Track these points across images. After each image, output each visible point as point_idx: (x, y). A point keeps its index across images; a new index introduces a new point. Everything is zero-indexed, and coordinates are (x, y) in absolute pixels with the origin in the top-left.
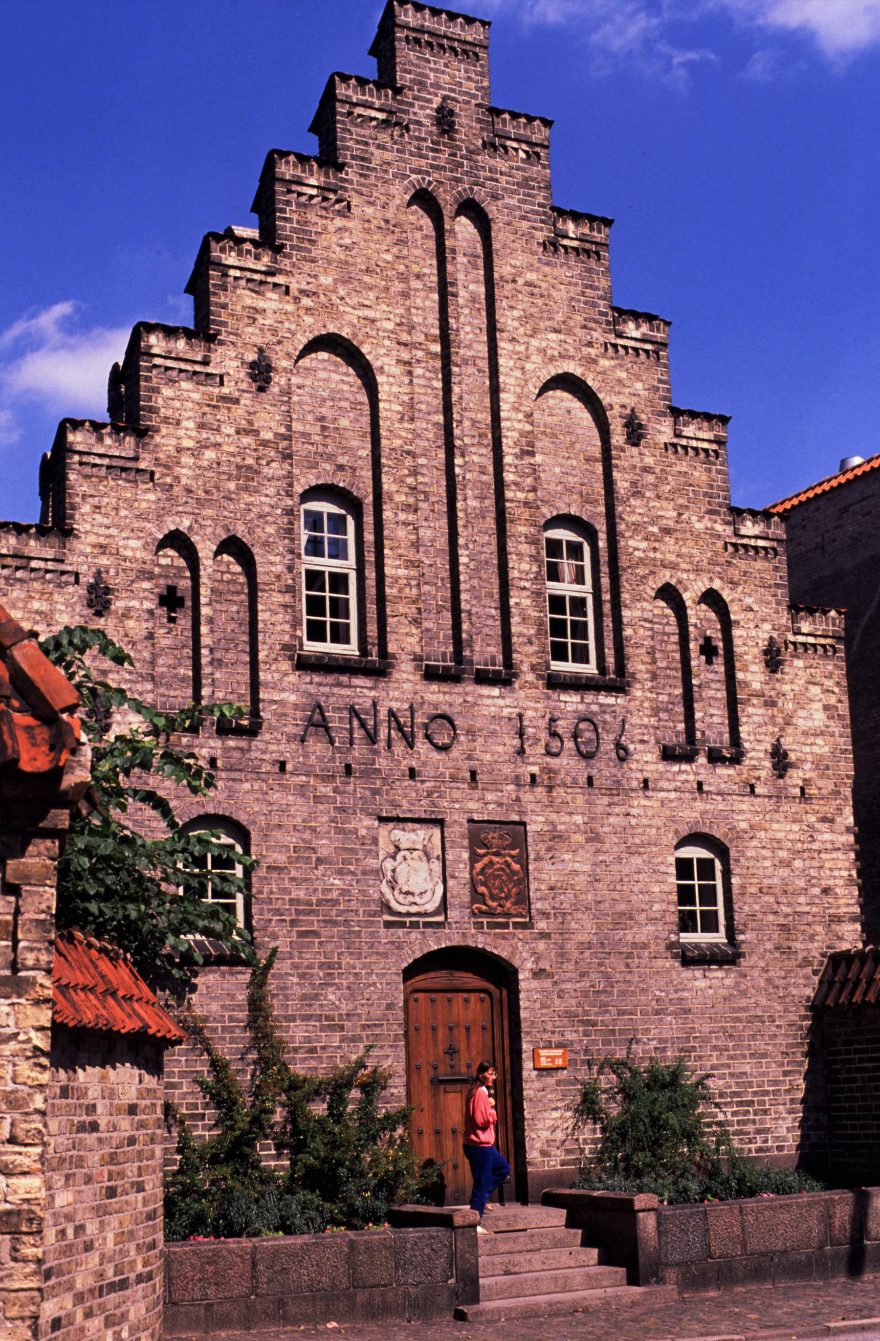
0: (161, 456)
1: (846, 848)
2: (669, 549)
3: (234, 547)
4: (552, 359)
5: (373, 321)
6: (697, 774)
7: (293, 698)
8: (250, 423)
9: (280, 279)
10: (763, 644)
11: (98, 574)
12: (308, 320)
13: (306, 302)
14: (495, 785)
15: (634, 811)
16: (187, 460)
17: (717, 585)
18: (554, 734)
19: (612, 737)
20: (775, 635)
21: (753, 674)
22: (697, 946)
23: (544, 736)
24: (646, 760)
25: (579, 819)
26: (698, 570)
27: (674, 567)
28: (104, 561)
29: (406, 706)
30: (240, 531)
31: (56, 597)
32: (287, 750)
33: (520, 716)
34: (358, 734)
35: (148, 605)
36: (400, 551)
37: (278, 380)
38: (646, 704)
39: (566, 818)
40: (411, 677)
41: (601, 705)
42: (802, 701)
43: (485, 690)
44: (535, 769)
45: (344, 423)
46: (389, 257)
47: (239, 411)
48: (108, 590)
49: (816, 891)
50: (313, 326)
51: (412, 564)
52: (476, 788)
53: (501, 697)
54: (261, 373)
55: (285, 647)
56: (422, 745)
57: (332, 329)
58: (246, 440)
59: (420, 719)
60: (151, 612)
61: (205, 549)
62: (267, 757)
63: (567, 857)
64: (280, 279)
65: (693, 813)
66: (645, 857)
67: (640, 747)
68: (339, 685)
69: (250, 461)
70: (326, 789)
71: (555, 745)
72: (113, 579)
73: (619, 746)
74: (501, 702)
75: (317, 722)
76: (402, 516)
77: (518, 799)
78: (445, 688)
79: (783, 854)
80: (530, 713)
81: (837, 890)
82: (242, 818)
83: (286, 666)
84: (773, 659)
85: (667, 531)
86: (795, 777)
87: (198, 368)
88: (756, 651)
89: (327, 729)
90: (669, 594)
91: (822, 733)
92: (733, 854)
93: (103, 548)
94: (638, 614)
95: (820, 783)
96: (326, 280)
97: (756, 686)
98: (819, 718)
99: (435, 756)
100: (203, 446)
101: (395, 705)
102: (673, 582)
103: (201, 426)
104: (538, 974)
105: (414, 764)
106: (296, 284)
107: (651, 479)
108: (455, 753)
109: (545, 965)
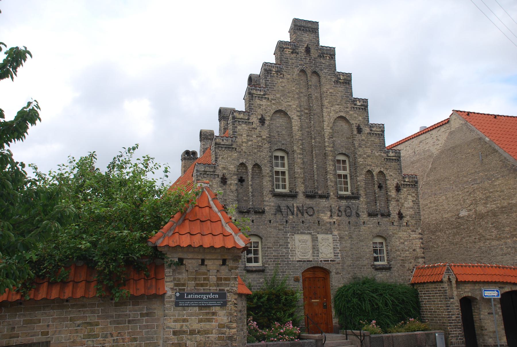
0: (238, 144)
2: (369, 161)
3: (257, 166)
4: (337, 112)
5: (290, 106)
7: (272, 204)
8: (260, 134)
9: (266, 96)
10: (395, 185)
11: (223, 175)
12: (274, 106)
13: (273, 102)
14: (324, 225)
15: (361, 230)
16: (244, 144)
17: (382, 170)
18: (340, 211)
21: (393, 193)
22: (379, 265)
23: (337, 212)
24: (364, 216)
25: (347, 233)
26: (377, 166)
27: (371, 165)
28: (225, 171)
30: (258, 162)
32: (272, 217)
34: (289, 213)
35: (236, 182)
37: (267, 123)
39: (343, 232)
42: (406, 199)
44: (335, 220)
45: (284, 132)
46: (294, 88)
47: (257, 131)
48: (226, 179)
49: (411, 250)
50: (275, 108)
51: (301, 168)
53: (326, 202)
54: (262, 121)
55: (270, 191)
56: (306, 215)
57: (280, 108)
58: (259, 139)
60: (236, 184)
61: (250, 167)
64: (266, 96)
68: (284, 200)
69: (260, 144)
70: (281, 227)
72: (228, 176)
75: (279, 210)
76: (299, 156)
77: (331, 228)
79: (402, 241)
80: (333, 206)
82: (260, 235)
83: (270, 196)
84: (398, 189)
85: (368, 156)
86: (405, 220)
87: (246, 121)
89: (281, 212)
90: (369, 172)
91: (412, 208)
92: (388, 241)
93: (224, 168)
95: (412, 221)
96: (278, 96)
99: (309, 217)
100: (248, 141)
104: (337, 273)
106: (271, 97)
107: (364, 142)
108: (314, 217)
109: (339, 271)
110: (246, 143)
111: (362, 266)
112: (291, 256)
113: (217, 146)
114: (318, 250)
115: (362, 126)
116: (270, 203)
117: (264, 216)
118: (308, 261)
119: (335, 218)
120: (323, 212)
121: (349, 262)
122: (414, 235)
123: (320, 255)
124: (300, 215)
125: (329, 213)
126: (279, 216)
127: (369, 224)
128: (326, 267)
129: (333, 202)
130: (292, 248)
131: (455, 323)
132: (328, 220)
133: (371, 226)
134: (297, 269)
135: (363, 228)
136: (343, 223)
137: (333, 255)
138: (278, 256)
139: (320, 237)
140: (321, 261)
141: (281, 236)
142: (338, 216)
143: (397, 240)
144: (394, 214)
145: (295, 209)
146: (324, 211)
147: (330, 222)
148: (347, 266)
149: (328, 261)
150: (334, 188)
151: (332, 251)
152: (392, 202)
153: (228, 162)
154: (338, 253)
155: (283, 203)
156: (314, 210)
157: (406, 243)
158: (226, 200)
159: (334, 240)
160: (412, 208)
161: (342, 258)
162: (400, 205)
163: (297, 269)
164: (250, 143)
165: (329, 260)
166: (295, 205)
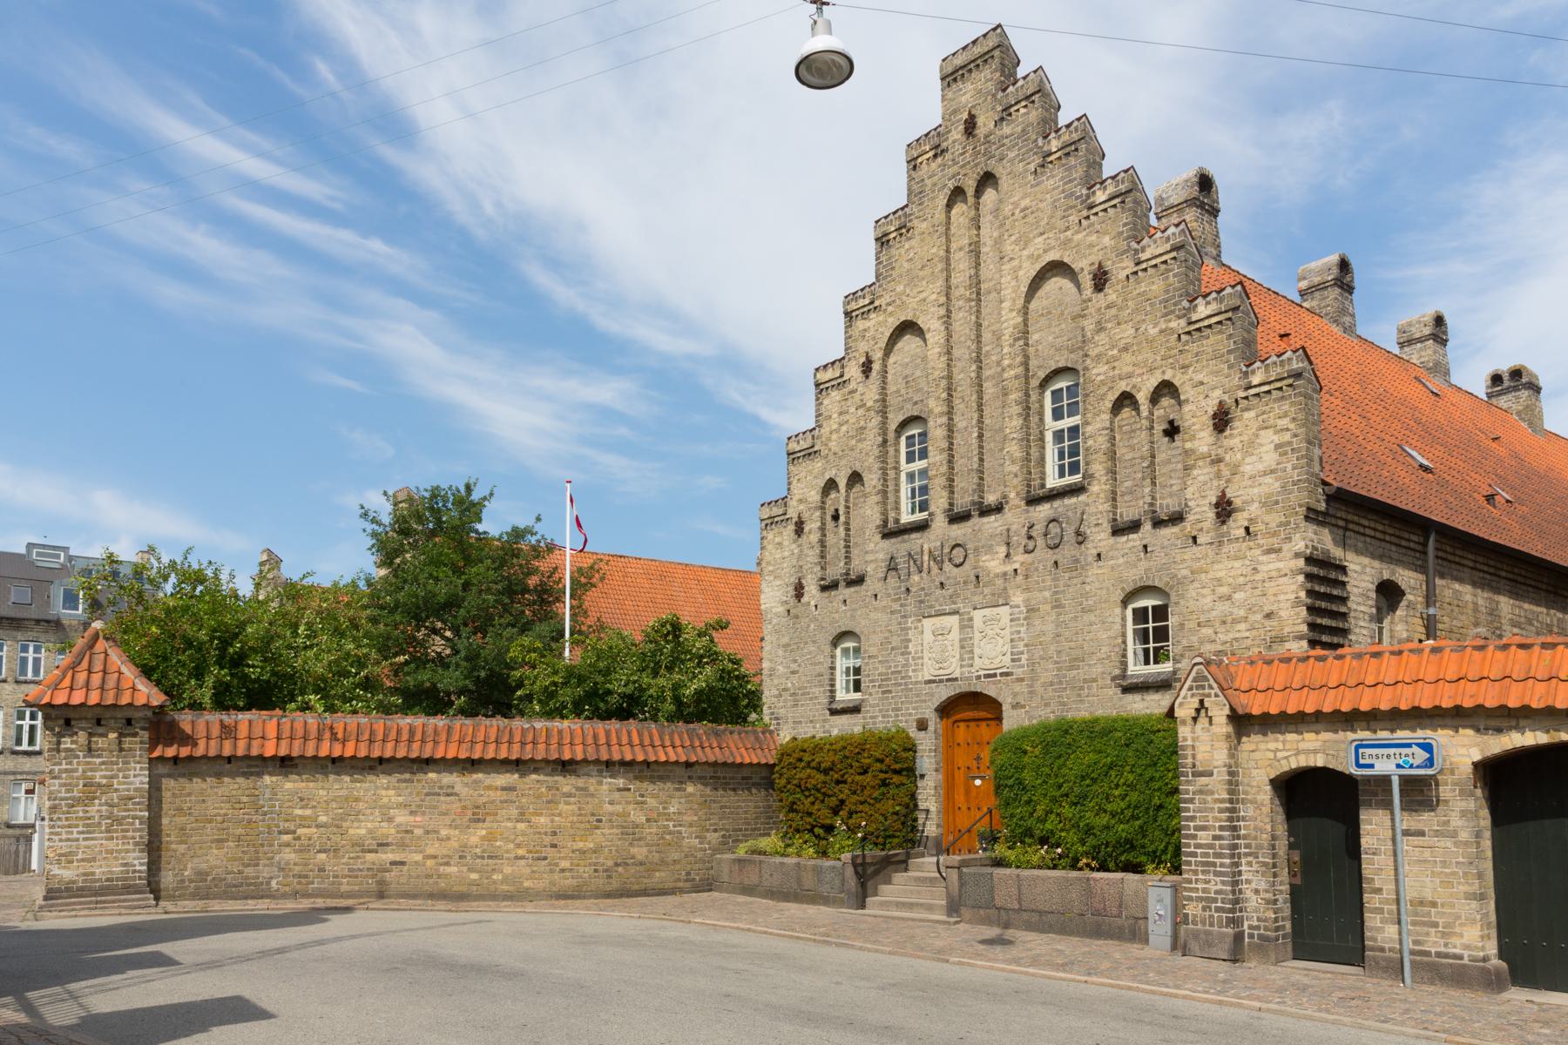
1: (1295, 573)
14: (990, 583)
18: (1030, 538)
20: (1226, 397)
23: (1024, 541)
24: (1100, 537)
25: (1047, 594)
27: (1129, 376)
39: (1038, 595)
43: (985, 520)
44: (1017, 566)
47: (857, 396)
49: (1258, 617)
56: (947, 566)
58: (861, 412)
59: (946, 550)
65: (1135, 575)
70: (896, 606)
71: (1031, 545)
72: (805, 516)
73: (1078, 533)
75: (892, 566)
78: (962, 525)
79: (1224, 590)
80: (1014, 527)
81: (1283, 614)
84: (1221, 420)
85: (1125, 349)
88: (1204, 418)
91: (1272, 472)
94: (1099, 426)
95: (1267, 518)
97: (1204, 449)
98: (1270, 458)
99: (956, 570)
104: (1016, 706)
108: (967, 566)
111: (1085, 681)
114: (972, 652)
116: (873, 553)
119: (1019, 558)
120: (990, 549)
121: (1047, 673)
122: (1270, 565)
123: (977, 662)
124: (935, 570)
125: (1003, 550)
126: (892, 581)
128: (991, 691)
129: (1015, 517)
132: (1001, 569)
133: (1121, 561)
135: (1095, 571)
137: (1008, 657)
139: (978, 616)
140: (979, 677)
141: (894, 628)
142: (1027, 552)
143: (1204, 591)
144: (1202, 511)
145: (926, 558)
147: (1005, 574)
148: (1044, 685)
149: (995, 675)
151: (1007, 648)
152: (1195, 472)
155: (899, 546)
157: (1238, 596)
160: (1272, 472)
162: (1226, 472)
164: (844, 428)
166: (926, 547)
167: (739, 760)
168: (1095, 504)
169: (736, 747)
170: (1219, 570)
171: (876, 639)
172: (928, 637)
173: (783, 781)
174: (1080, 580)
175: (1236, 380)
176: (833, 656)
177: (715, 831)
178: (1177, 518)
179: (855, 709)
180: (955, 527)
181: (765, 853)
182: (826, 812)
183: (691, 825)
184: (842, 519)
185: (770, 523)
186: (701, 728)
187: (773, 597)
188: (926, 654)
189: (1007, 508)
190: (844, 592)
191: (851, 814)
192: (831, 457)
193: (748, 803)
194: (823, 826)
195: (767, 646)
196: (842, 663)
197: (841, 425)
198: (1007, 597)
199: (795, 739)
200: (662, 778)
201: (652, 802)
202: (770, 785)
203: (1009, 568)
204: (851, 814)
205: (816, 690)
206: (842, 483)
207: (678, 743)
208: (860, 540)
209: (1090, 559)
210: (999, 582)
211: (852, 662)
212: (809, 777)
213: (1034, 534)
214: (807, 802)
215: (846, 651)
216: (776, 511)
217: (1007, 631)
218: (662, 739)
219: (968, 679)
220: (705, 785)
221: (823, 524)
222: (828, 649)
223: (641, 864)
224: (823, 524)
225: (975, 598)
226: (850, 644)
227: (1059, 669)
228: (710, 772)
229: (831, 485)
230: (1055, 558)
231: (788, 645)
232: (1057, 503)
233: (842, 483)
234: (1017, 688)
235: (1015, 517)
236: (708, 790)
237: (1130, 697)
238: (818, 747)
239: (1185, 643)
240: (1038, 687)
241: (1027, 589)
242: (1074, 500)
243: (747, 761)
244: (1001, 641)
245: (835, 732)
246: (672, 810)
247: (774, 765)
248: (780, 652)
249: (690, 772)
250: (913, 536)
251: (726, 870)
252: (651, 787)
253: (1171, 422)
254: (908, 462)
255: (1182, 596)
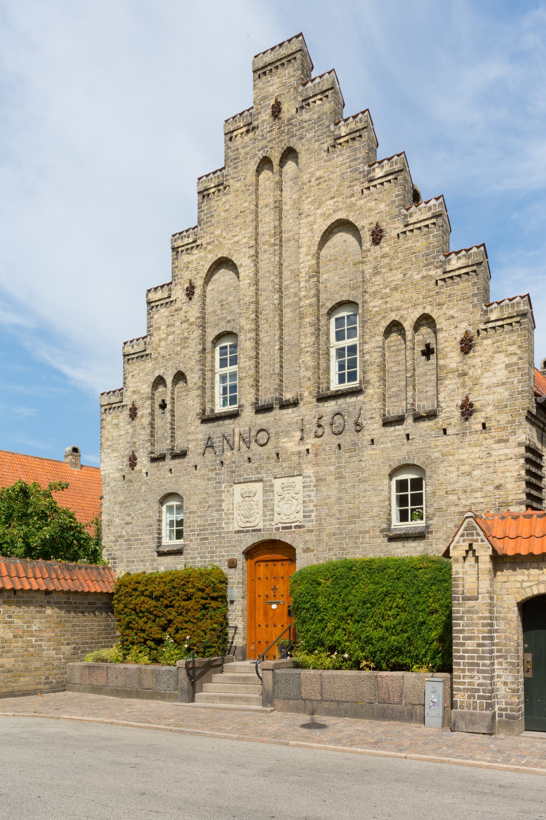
1: (518, 457)
4: (330, 215)
5: (238, 242)
6: (405, 430)
8: (186, 317)
9: (199, 242)
13: (210, 247)
14: (288, 459)
15: (364, 459)
18: (319, 426)
19: (353, 420)
20: (470, 328)
23: (315, 428)
24: (374, 428)
25: (332, 468)
28: (135, 397)
29: (247, 428)
31: (120, 417)
33: (302, 420)
34: (226, 446)
36: (247, 353)
38: (375, 397)
39: (325, 469)
40: (250, 414)
41: (349, 403)
43: (284, 411)
44: (309, 447)
47: (182, 313)
49: (491, 488)
52: (279, 462)
53: (293, 412)
54: (190, 292)
56: (254, 446)
57: (220, 255)
58: (185, 325)
59: (253, 433)
62: (190, 465)
63: (324, 489)
66: (370, 483)
67: (369, 422)
69: (186, 334)
70: (212, 475)
72: (138, 404)
73: (357, 424)
74: (293, 415)
75: (209, 445)
77: (299, 463)
78: (266, 415)
79: (466, 468)
80: (307, 418)
81: (508, 486)
84: (467, 345)
87: (167, 300)
88: (454, 343)
91: (503, 384)
93: (134, 392)
94: (374, 345)
96: (218, 232)
97: (454, 366)
98: (502, 374)
99: (260, 449)
101: (242, 430)
102: (397, 319)
103: (168, 326)
105: (250, 456)
107: (387, 260)
108: (269, 446)
110: (165, 339)
111: (360, 532)
112: (226, 523)
113: (127, 358)
114: (272, 510)
115: (383, 225)
116: (193, 434)
117: (186, 459)
118: (254, 531)
119: (310, 442)
120: (287, 434)
121: (331, 526)
122: (500, 451)
123: (277, 518)
124: (244, 448)
125: (298, 435)
126: (209, 455)
127: (383, 443)
128: (287, 539)
129: (308, 410)
130: (228, 510)
131: (472, 658)
132: (296, 449)
133: (389, 445)
134: (235, 546)
135: (369, 452)
136: (324, 450)
137: (301, 514)
138: (205, 525)
140: (278, 529)
142: (316, 436)
143: (451, 469)
144: (450, 410)
145: (237, 439)
146: (289, 431)
147: (299, 452)
149: (290, 527)
150: (312, 382)
151: (301, 507)
152: (446, 382)
153: (139, 381)
154: (312, 511)
155: (216, 430)
156: (269, 434)
157: (476, 473)
158: (135, 443)
159: (304, 487)
160: (503, 384)
161: (319, 519)
162: (469, 383)
163: (235, 546)
164: (171, 338)
165: (293, 525)
166: (237, 431)
167: (86, 590)
168: (370, 404)
169: (82, 579)
170: (463, 454)
171: (196, 499)
172: (237, 498)
173: (121, 606)
174: (357, 458)
175: (478, 316)
176: (160, 512)
177: (68, 644)
178: (432, 415)
179: (179, 552)
180: (260, 416)
181: (106, 661)
182: (156, 629)
183: (49, 640)
184: (169, 407)
185: (109, 408)
186: (55, 563)
187: (111, 465)
188: (235, 512)
189: (301, 403)
190: (169, 463)
191: (177, 631)
192: (160, 359)
193: (93, 623)
194: (153, 640)
195: (106, 503)
196: (166, 518)
197: (168, 335)
198: (301, 470)
199: (128, 574)
200: (27, 603)
201: (18, 622)
202: (109, 609)
203: (303, 448)
204: (177, 631)
205: (146, 538)
206: (169, 380)
207: (39, 575)
208: (182, 424)
209: (365, 443)
210: (295, 458)
211: (175, 517)
212: (143, 602)
213: (323, 423)
214: (141, 622)
215: (170, 509)
216: (114, 399)
217: (300, 496)
218: (26, 572)
219: (268, 530)
220: (61, 608)
221: (153, 411)
222: (156, 506)
223: (9, 671)
224: (153, 411)
225: (276, 470)
226: (174, 503)
227: (340, 524)
228: (64, 598)
229: (160, 381)
230: (338, 441)
231: (123, 502)
232: (341, 401)
233: (169, 380)
234: (308, 537)
235: (308, 410)
236: (63, 613)
237: (394, 544)
238: (150, 580)
239: (436, 505)
240: (324, 536)
241: (317, 464)
242: (354, 399)
243: (93, 590)
244: (295, 502)
245: (162, 569)
246: (34, 628)
247: (113, 594)
248: (117, 508)
249: (48, 598)
250: (227, 422)
251: (77, 674)
252: (17, 610)
253: (428, 346)
254: (221, 366)
255: (435, 472)
